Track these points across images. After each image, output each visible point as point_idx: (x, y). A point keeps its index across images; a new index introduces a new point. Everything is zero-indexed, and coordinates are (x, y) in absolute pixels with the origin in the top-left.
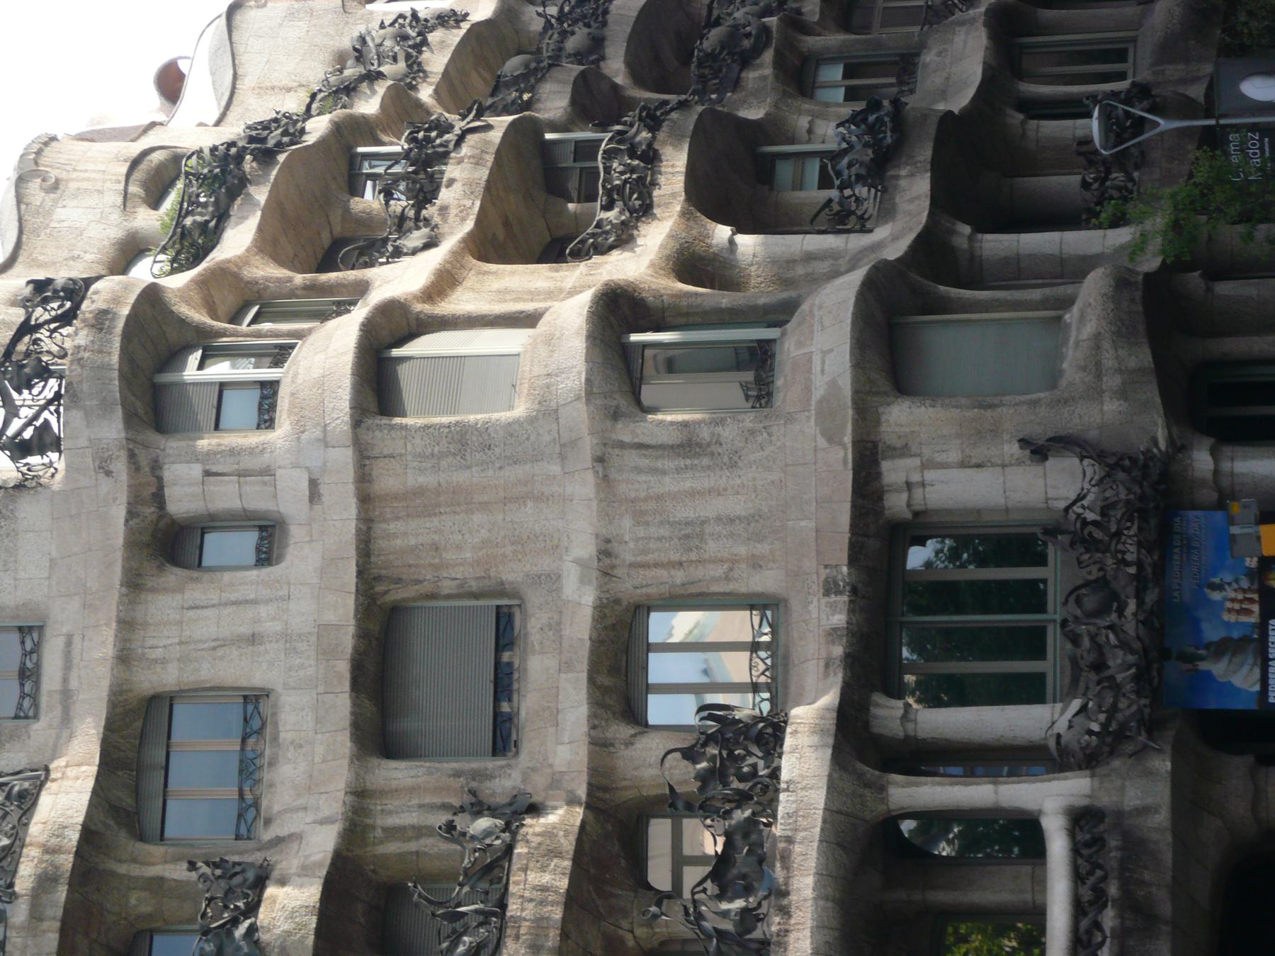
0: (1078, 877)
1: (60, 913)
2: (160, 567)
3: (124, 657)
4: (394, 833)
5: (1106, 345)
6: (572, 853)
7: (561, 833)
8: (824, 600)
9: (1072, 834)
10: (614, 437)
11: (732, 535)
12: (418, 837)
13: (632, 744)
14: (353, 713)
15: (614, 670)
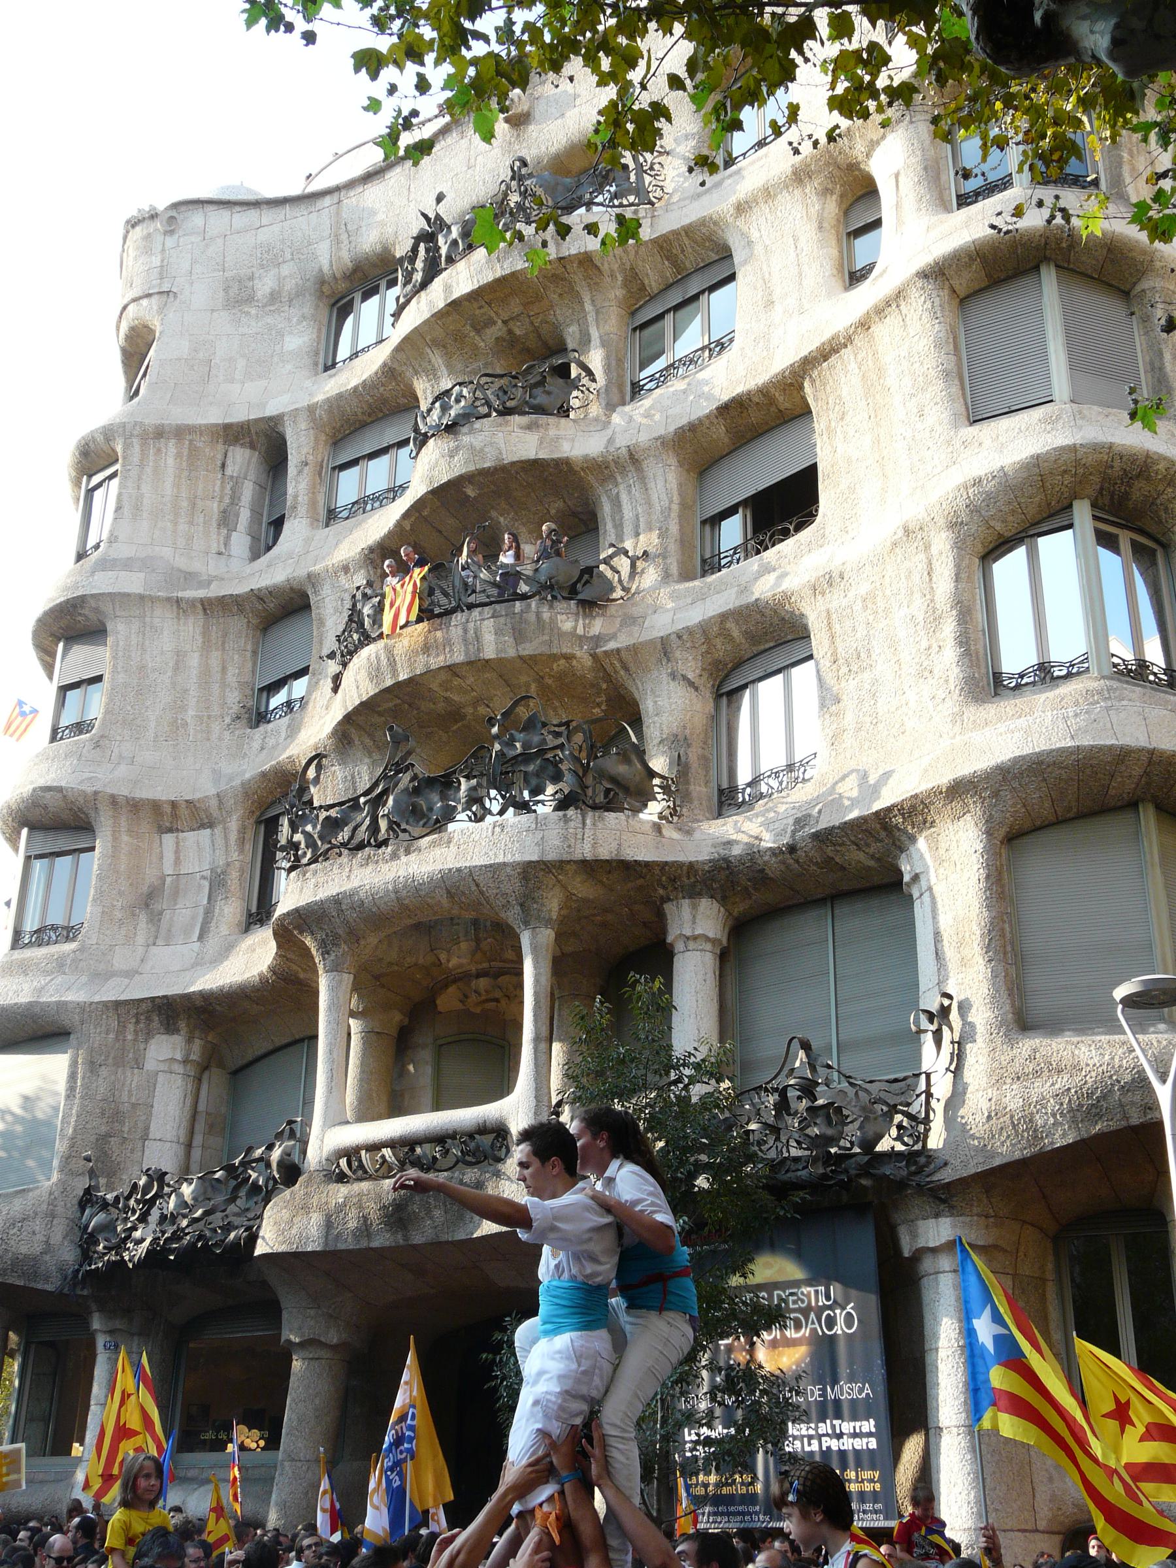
0: (440, 1138)
1: (508, 271)
2: (825, 192)
3: (741, 208)
4: (617, 503)
5: (1063, 1082)
6: (526, 653)
7: (546, 638)
8: (791, 821)
9: (483, 1129)
10: (932, 534)
11: (861, 701)
12: (615, 526)
13: (674, 679)
14: (700, 419)
15: (752, 638)
